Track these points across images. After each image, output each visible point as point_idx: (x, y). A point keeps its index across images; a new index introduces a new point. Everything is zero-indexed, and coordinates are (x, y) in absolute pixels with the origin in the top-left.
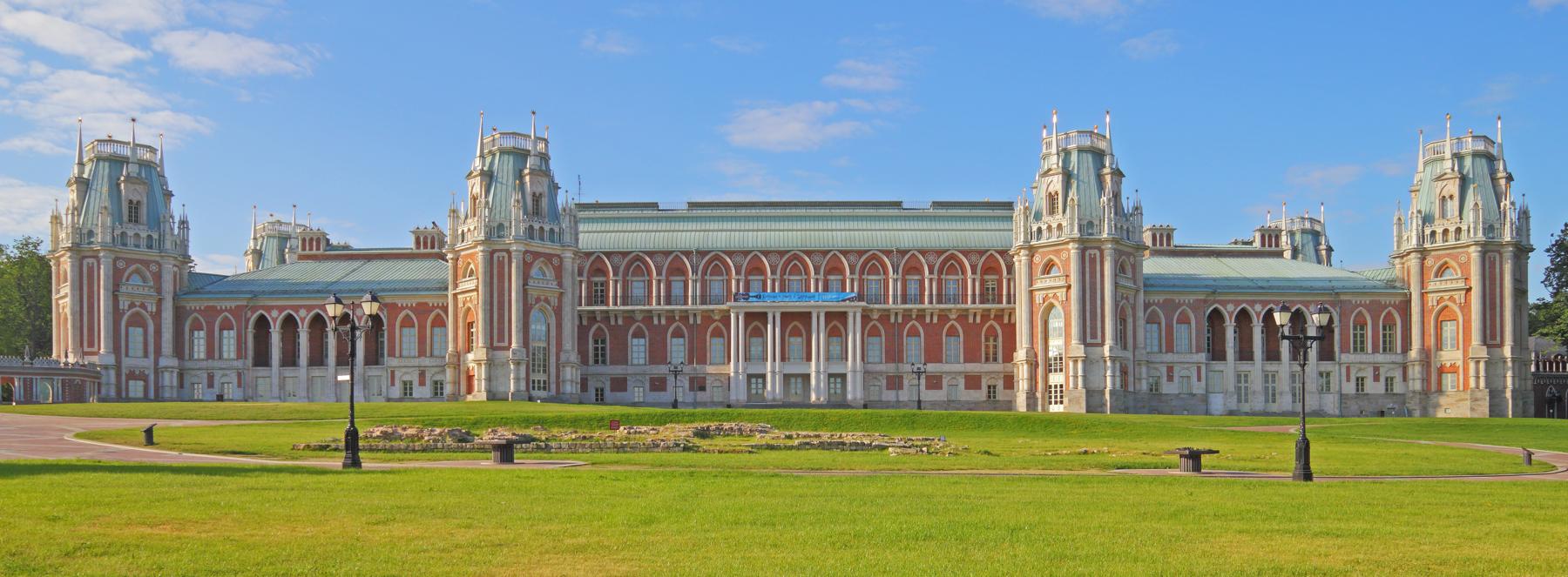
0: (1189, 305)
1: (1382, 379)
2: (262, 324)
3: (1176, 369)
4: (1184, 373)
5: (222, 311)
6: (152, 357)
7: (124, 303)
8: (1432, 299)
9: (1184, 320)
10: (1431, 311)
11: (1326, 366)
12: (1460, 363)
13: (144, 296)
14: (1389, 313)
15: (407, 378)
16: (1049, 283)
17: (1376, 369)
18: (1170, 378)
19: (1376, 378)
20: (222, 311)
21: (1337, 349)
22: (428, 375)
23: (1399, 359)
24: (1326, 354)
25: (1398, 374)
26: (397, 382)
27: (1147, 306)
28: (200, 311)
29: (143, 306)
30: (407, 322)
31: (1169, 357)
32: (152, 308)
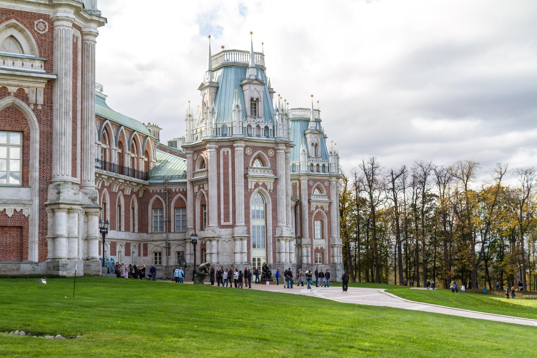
10: (313, 213)
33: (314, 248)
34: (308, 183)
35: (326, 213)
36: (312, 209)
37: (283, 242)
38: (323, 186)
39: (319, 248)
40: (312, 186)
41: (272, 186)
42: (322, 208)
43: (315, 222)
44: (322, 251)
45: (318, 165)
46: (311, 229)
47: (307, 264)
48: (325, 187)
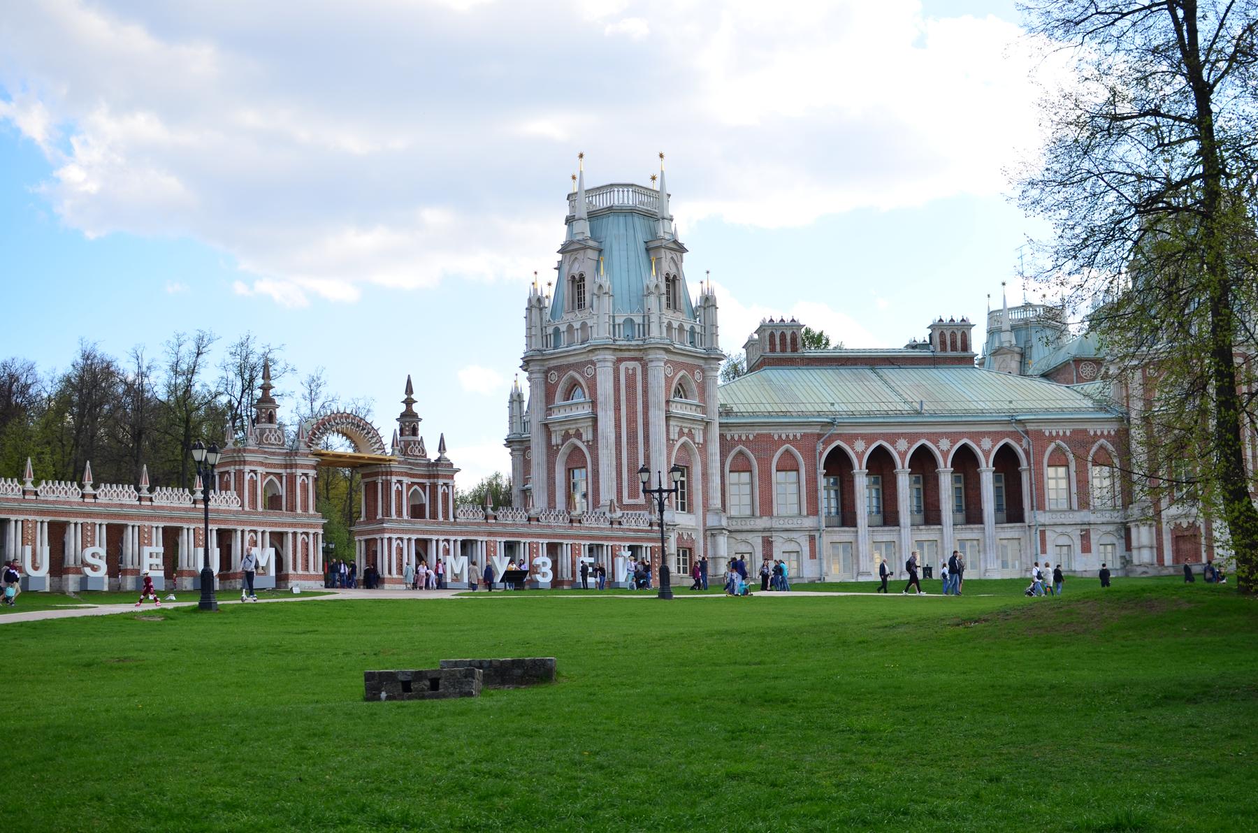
2: (838, 464)
5: (781, 442)
6: (699, 510)
7: (674, 435)
13: (694, 420)
15: (1064, 540)
20: (781, 442)
22: (1094, 537)
26: (1049, 547)
28: (747, 442)
29: (691, 435)
30: (1058, 460)
32: (699, 438)
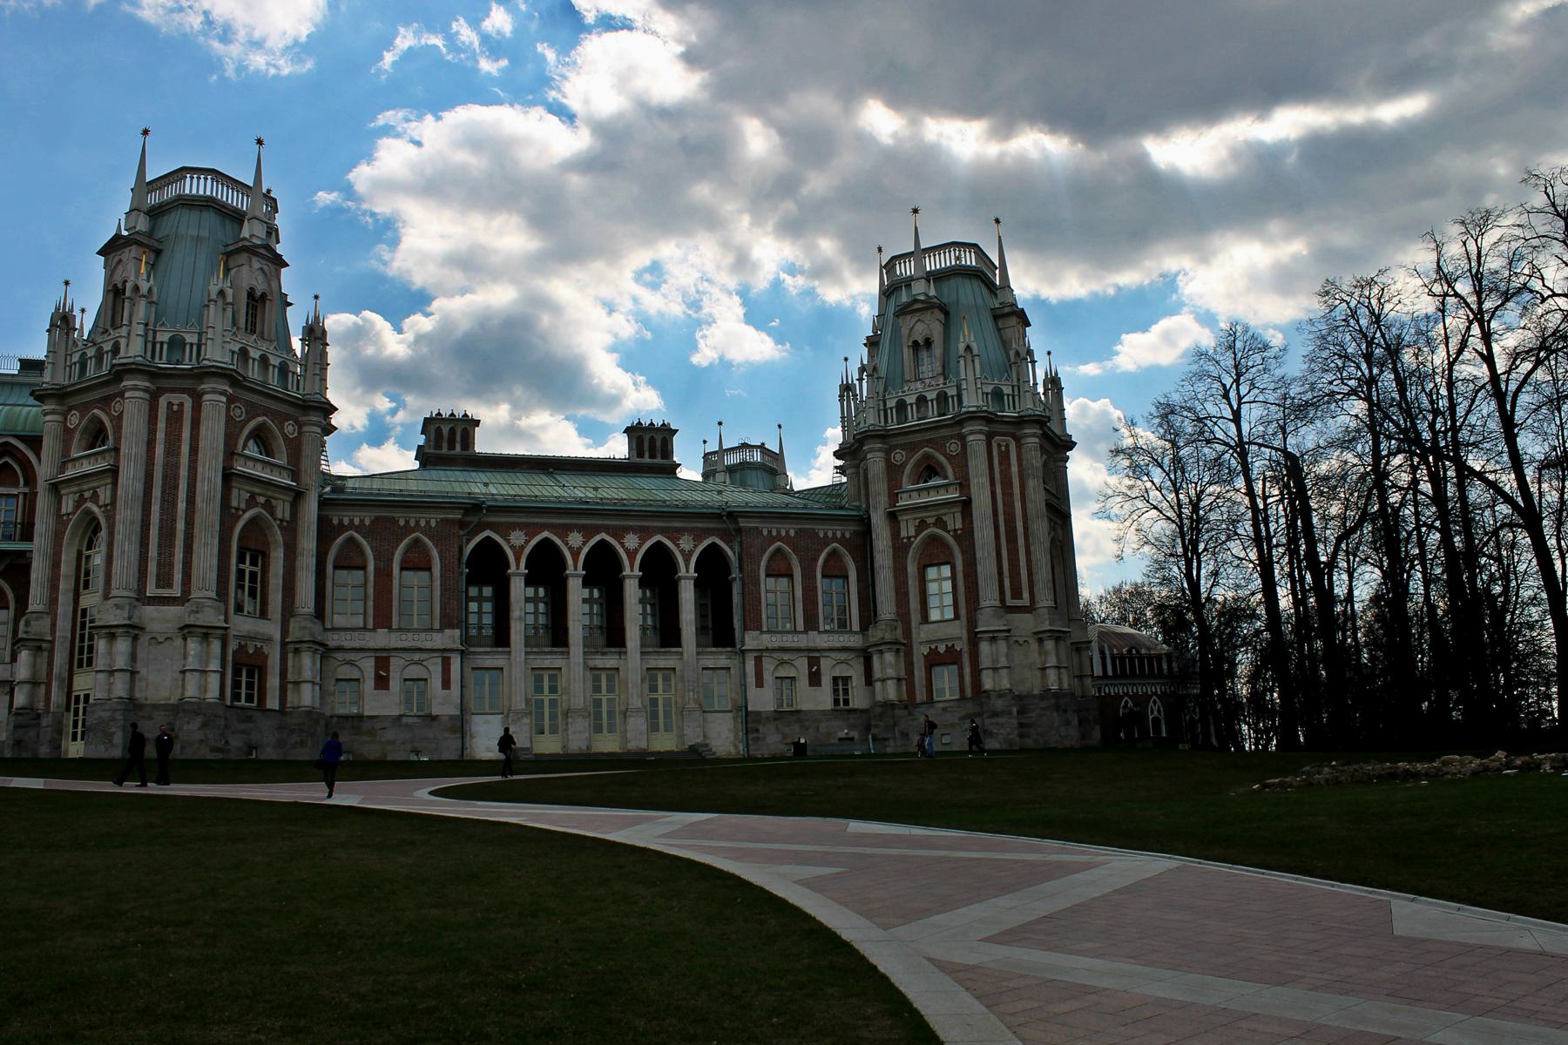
0: (428, 531)
1: (826, 681)
3: (396, 663)
4: (415, 671)
8: (908, 528)
9: (416, 562)
11: (720, 658)
12: (962, 646)
14: (834, 553)
16: (87, 467)
17: (813, 662)
18: (382, 682)
19: (815, 679)
21: (737, 624)
23: (855, 641)
24: (719, 632)
25: (855, 671)
27: (326, 532)
31: (381, 639)
33: (920, 651)
34: (888, 460)
35: (956, 537)
36: (903, 534)
37: (101, 645)
38: (942, 458)
39: (942, 649)
40: (903, 465)
41: (108, 493)
42: (940, 523)
43: (932, 573)
44: (952, 657)
45: (922, 400)
46: (907, 594)
47: (888, 705)
48: (949, 458)
